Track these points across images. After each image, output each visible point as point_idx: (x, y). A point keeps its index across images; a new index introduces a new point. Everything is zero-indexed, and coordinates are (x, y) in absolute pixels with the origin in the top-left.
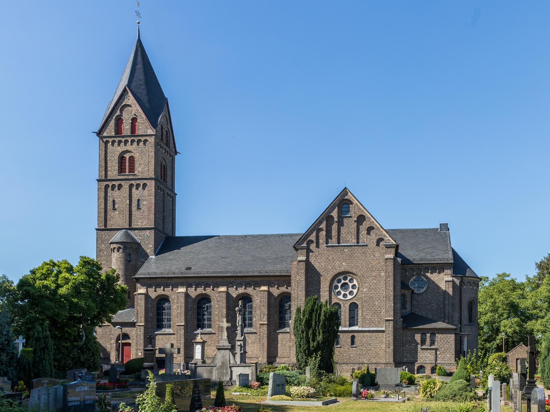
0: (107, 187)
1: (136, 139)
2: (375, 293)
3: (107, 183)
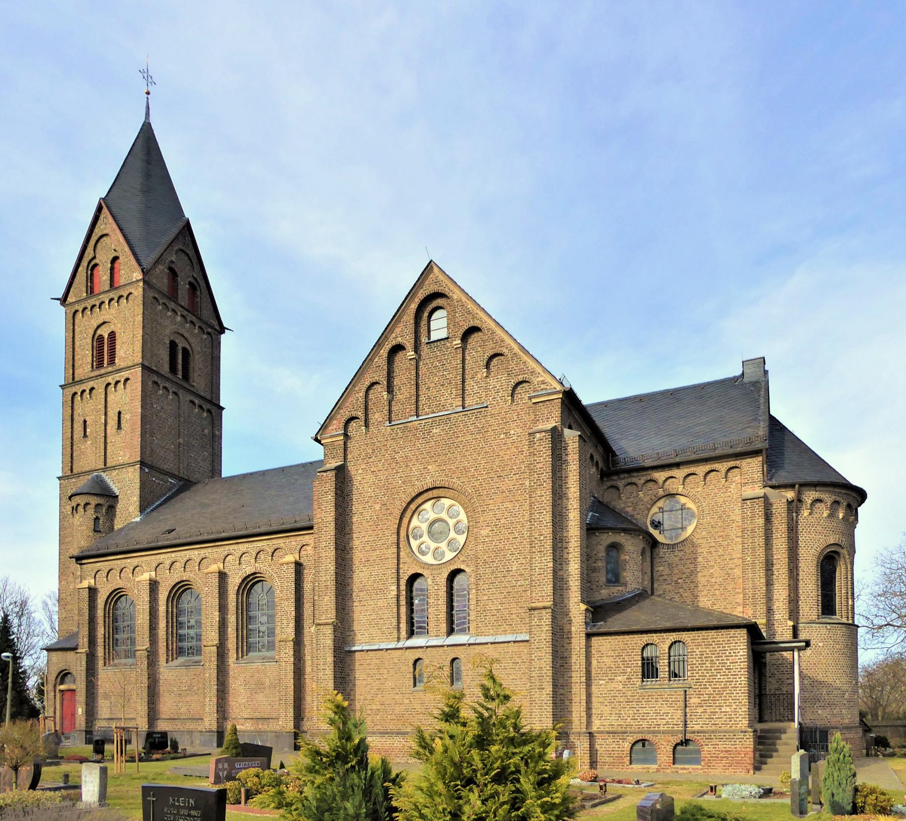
2: (511, 537)
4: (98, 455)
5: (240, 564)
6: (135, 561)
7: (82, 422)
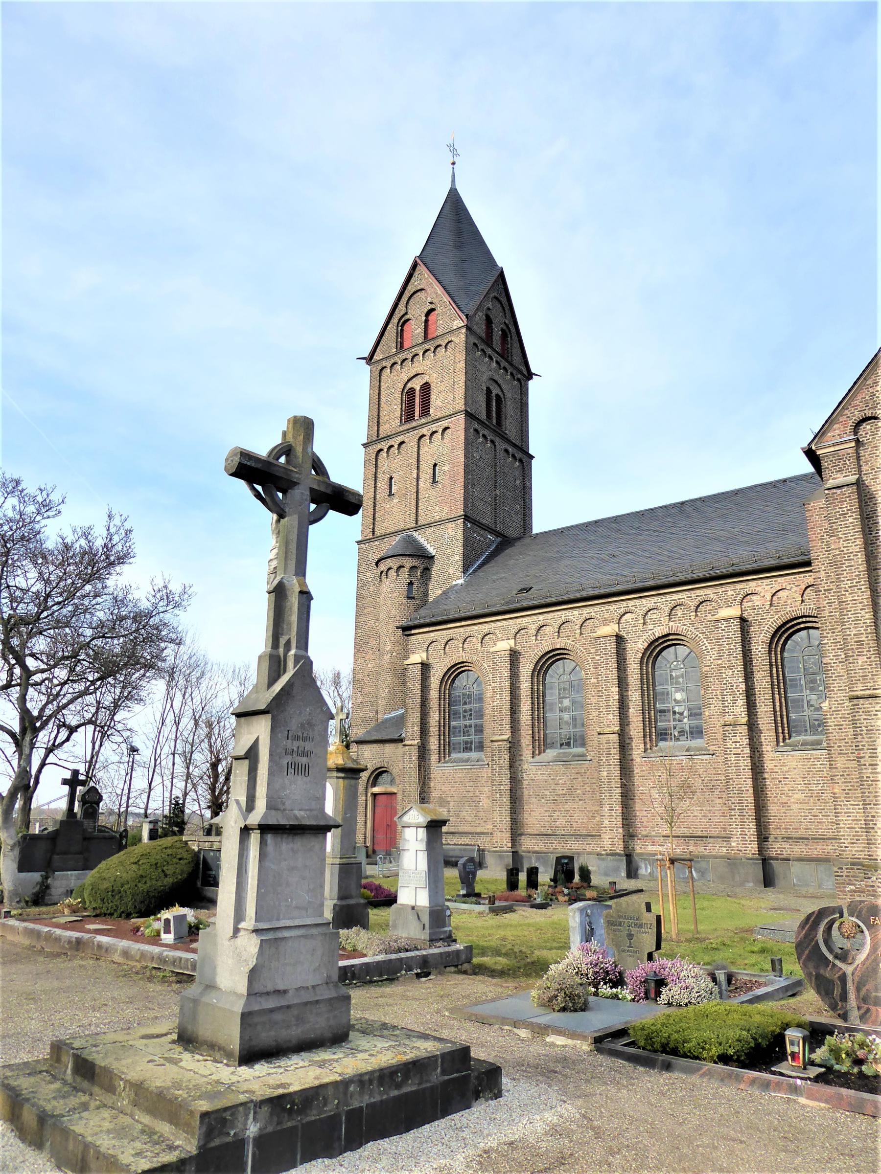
4: (407, 513)
5: (644, 623)
6: (485, 628)
7: (387, 479)
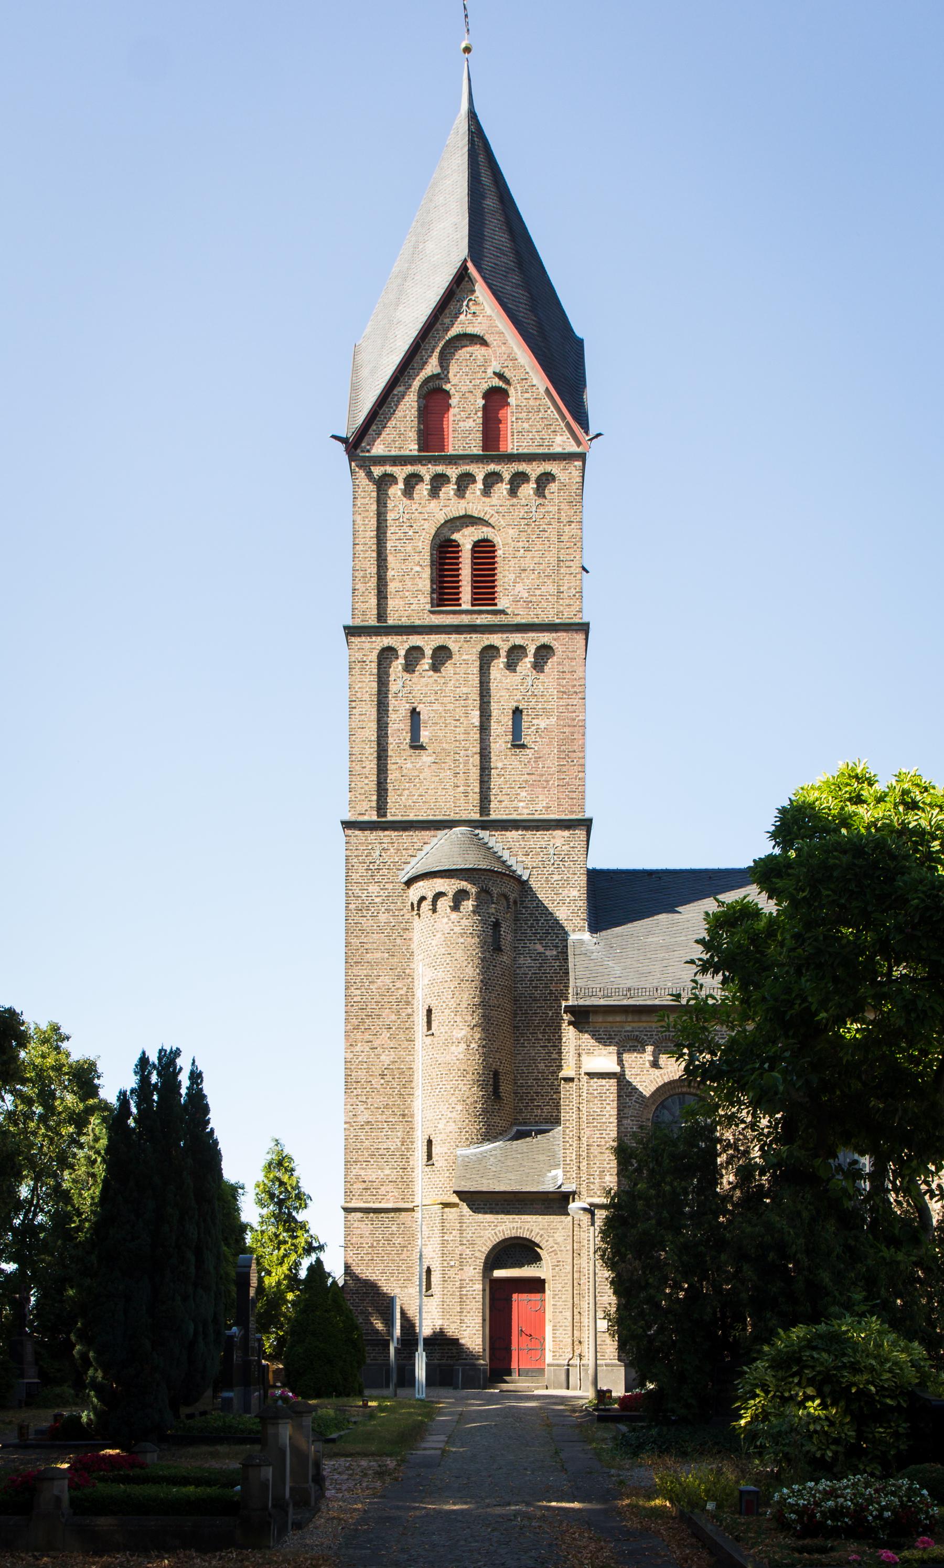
0: (387, 654)
1: (507, 471)
3: (387, 641)
